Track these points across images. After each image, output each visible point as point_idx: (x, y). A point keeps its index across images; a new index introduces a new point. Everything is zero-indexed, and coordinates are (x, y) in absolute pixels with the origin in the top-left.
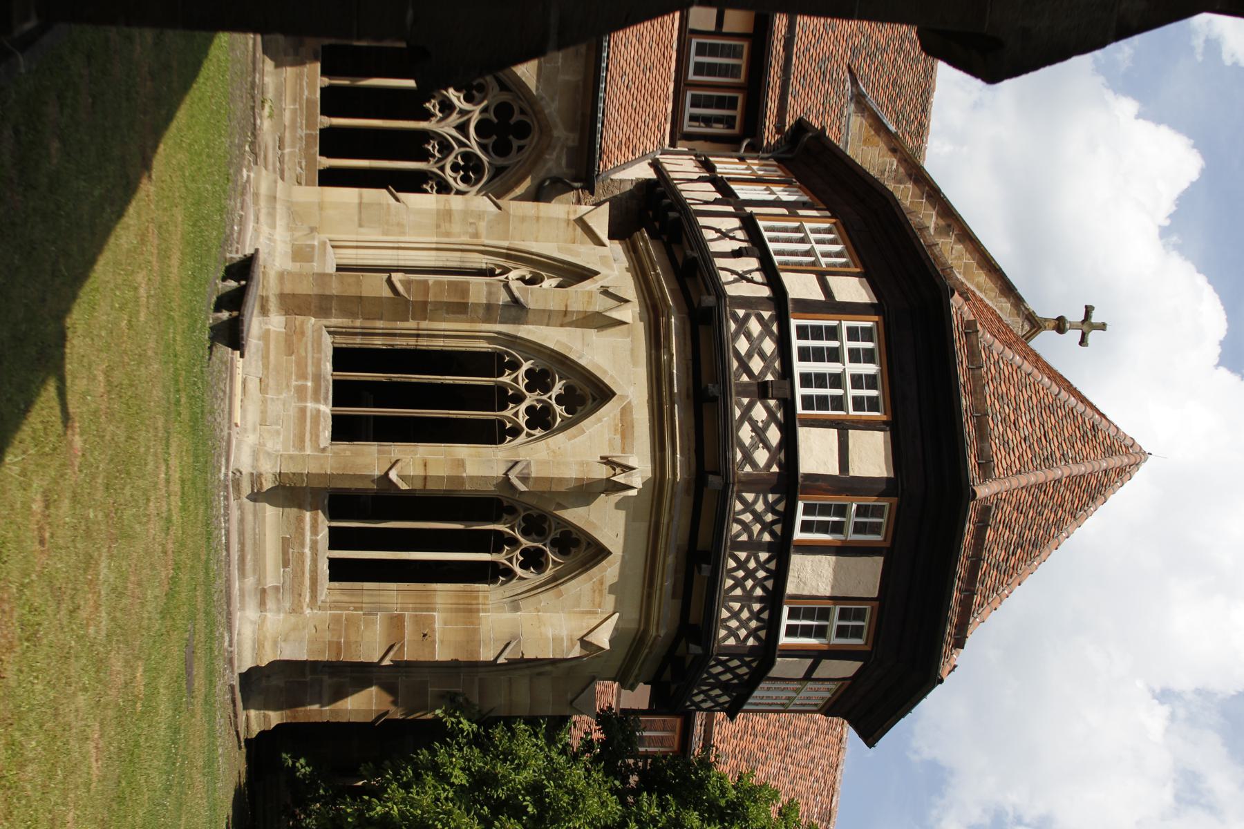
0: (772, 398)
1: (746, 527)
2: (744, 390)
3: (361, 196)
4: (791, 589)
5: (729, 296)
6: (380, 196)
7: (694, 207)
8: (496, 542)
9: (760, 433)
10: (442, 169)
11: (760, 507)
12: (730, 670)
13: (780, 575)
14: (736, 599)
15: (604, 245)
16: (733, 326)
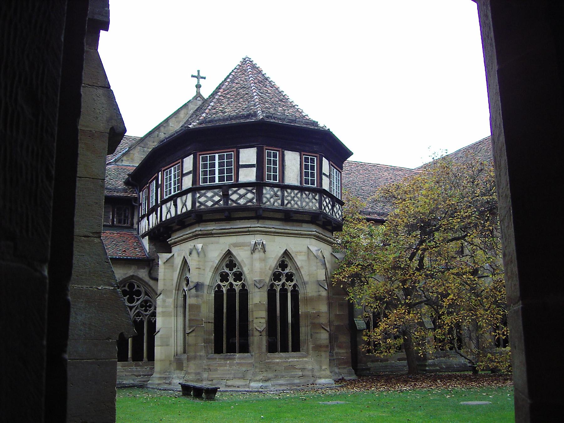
0: (228, 192)
2: (226, 203)
3: (158, 346)
4: (297, 184)
5: (192, 209)
6: (157, 338)
7: (159, 222)
8: (284, 291)
9: (241, 197)
10: (146, 315)
12: (327, 205)
13: (293, 188)
14: (301, 203)
15: (174, 255)
16: (203, 207)
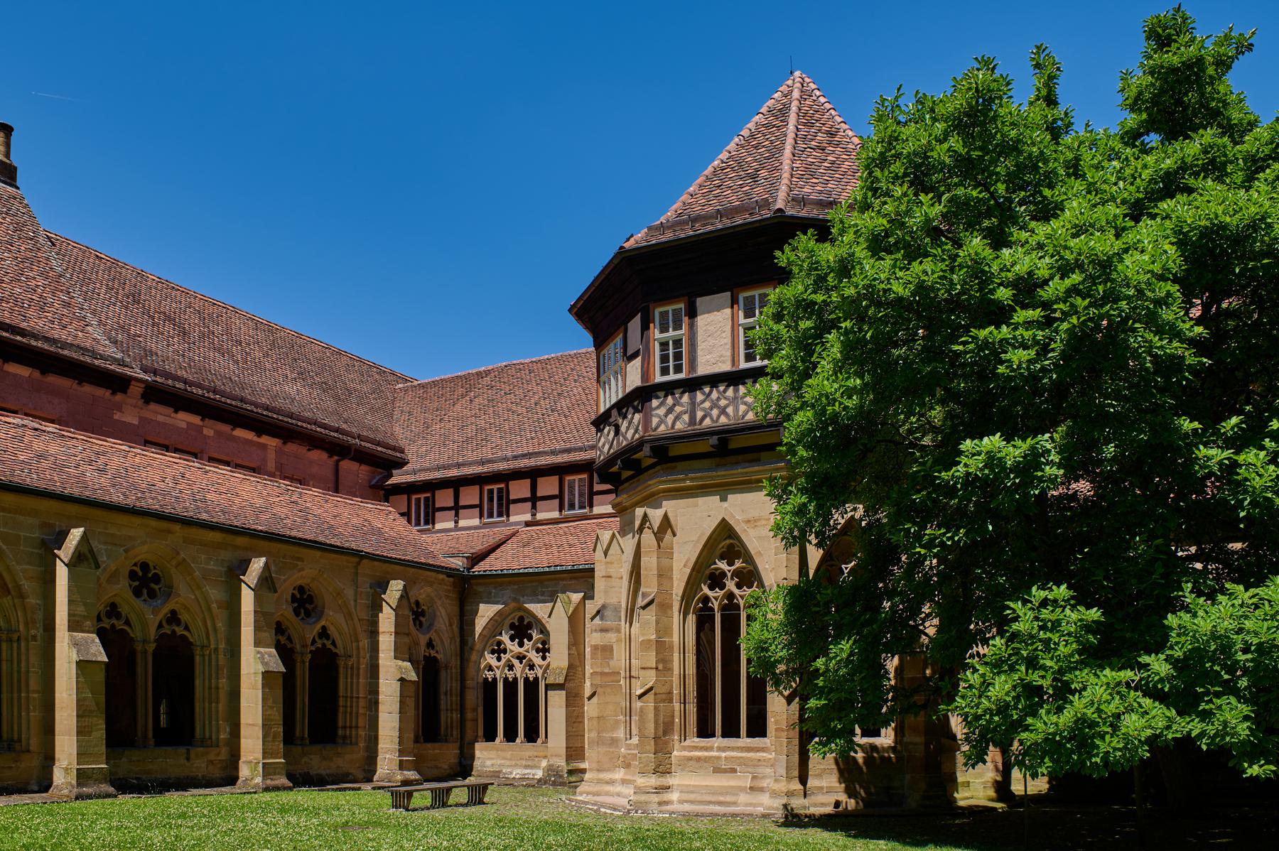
1: (677, 418)
11: (662, 411)
13: (714, 380)
